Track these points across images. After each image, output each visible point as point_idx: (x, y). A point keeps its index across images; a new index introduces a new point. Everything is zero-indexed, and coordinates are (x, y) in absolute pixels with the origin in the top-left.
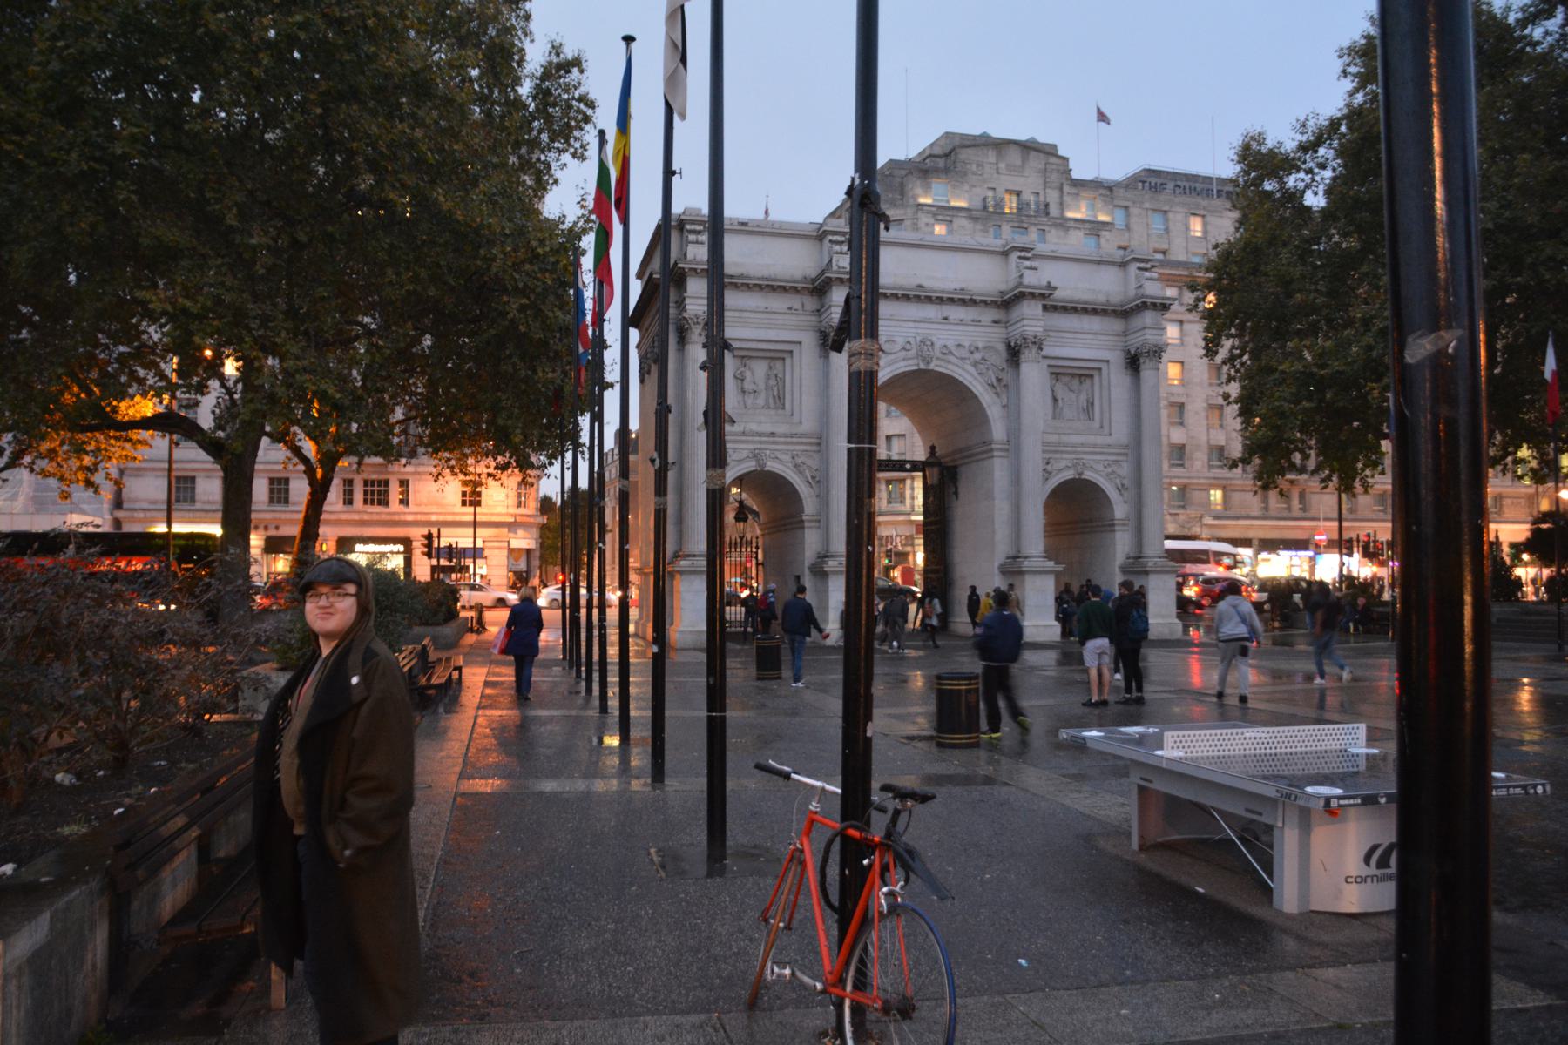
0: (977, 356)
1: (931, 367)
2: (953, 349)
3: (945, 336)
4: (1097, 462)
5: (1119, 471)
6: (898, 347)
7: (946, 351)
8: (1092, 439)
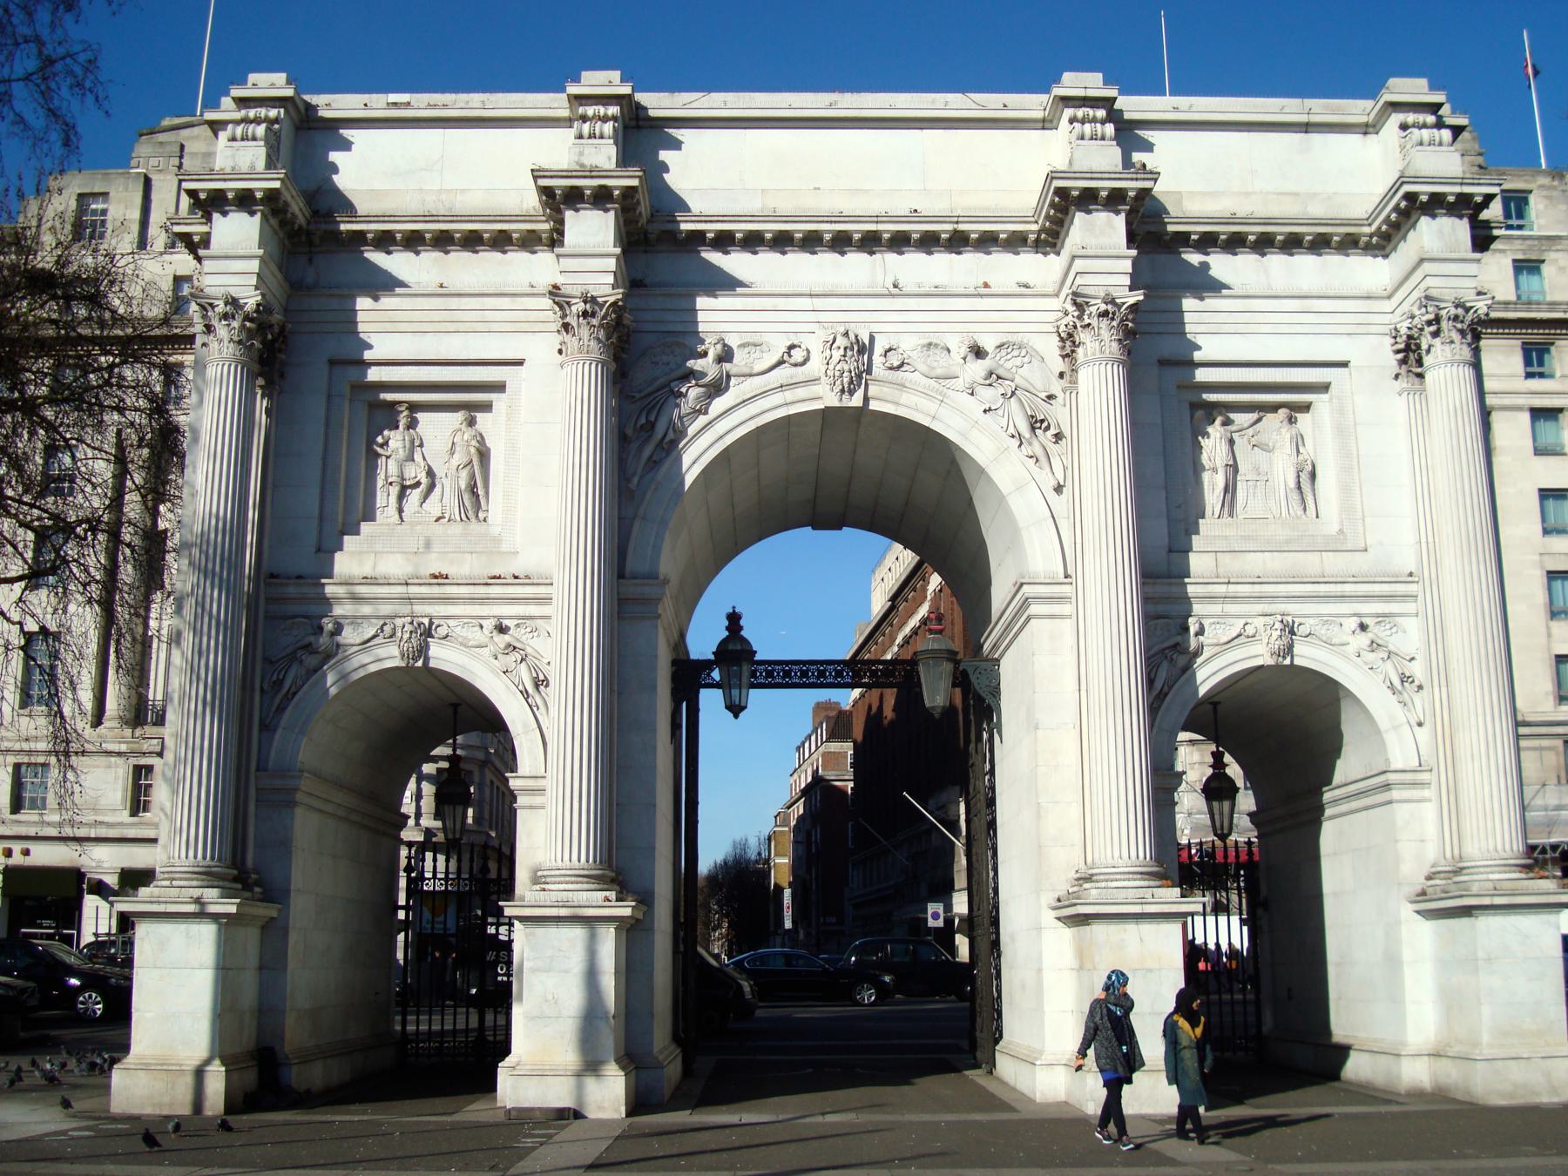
0: (978, 368)
1: (856, 401)
2: (916, 358)
3: (896, 330)
4: (1328, 620)
5: (1395, 642)
8: (1311, 563)
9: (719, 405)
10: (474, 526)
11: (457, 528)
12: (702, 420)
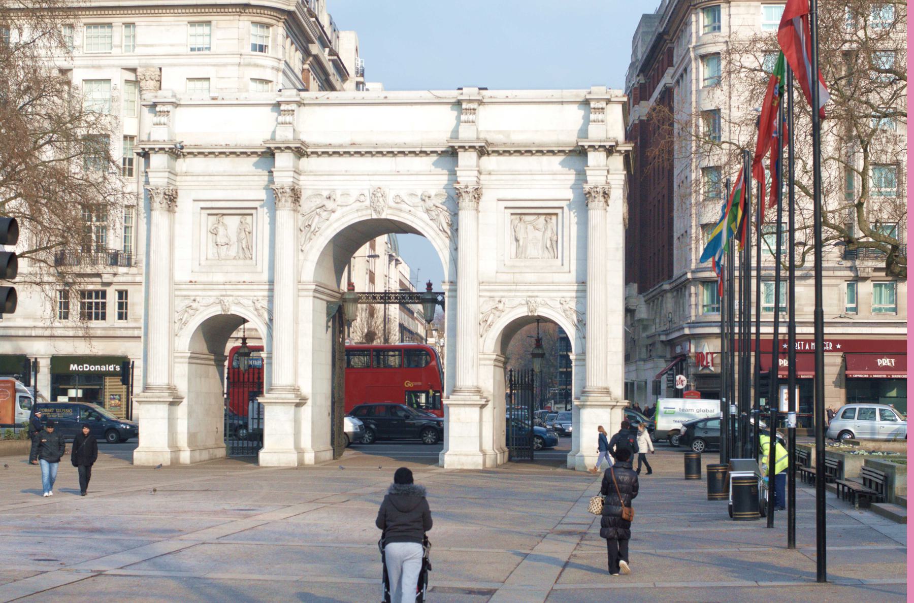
1: (383, 216)
2: (406, 199)
4: (552, 299)
6: (352, 200)
7: (399, 200)
9: (334, 216)
10: (248, 262)
11: (241, 262)
12: (328, 222)
